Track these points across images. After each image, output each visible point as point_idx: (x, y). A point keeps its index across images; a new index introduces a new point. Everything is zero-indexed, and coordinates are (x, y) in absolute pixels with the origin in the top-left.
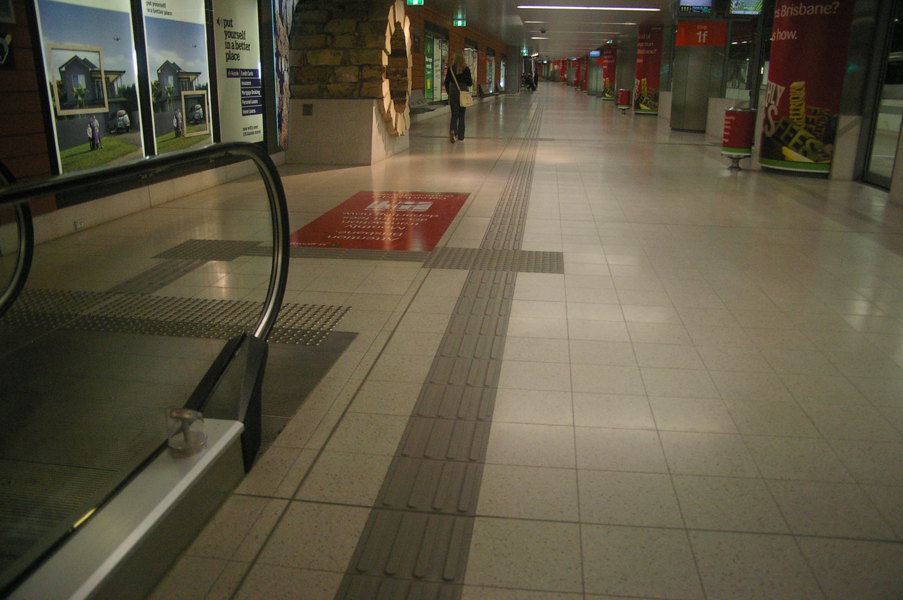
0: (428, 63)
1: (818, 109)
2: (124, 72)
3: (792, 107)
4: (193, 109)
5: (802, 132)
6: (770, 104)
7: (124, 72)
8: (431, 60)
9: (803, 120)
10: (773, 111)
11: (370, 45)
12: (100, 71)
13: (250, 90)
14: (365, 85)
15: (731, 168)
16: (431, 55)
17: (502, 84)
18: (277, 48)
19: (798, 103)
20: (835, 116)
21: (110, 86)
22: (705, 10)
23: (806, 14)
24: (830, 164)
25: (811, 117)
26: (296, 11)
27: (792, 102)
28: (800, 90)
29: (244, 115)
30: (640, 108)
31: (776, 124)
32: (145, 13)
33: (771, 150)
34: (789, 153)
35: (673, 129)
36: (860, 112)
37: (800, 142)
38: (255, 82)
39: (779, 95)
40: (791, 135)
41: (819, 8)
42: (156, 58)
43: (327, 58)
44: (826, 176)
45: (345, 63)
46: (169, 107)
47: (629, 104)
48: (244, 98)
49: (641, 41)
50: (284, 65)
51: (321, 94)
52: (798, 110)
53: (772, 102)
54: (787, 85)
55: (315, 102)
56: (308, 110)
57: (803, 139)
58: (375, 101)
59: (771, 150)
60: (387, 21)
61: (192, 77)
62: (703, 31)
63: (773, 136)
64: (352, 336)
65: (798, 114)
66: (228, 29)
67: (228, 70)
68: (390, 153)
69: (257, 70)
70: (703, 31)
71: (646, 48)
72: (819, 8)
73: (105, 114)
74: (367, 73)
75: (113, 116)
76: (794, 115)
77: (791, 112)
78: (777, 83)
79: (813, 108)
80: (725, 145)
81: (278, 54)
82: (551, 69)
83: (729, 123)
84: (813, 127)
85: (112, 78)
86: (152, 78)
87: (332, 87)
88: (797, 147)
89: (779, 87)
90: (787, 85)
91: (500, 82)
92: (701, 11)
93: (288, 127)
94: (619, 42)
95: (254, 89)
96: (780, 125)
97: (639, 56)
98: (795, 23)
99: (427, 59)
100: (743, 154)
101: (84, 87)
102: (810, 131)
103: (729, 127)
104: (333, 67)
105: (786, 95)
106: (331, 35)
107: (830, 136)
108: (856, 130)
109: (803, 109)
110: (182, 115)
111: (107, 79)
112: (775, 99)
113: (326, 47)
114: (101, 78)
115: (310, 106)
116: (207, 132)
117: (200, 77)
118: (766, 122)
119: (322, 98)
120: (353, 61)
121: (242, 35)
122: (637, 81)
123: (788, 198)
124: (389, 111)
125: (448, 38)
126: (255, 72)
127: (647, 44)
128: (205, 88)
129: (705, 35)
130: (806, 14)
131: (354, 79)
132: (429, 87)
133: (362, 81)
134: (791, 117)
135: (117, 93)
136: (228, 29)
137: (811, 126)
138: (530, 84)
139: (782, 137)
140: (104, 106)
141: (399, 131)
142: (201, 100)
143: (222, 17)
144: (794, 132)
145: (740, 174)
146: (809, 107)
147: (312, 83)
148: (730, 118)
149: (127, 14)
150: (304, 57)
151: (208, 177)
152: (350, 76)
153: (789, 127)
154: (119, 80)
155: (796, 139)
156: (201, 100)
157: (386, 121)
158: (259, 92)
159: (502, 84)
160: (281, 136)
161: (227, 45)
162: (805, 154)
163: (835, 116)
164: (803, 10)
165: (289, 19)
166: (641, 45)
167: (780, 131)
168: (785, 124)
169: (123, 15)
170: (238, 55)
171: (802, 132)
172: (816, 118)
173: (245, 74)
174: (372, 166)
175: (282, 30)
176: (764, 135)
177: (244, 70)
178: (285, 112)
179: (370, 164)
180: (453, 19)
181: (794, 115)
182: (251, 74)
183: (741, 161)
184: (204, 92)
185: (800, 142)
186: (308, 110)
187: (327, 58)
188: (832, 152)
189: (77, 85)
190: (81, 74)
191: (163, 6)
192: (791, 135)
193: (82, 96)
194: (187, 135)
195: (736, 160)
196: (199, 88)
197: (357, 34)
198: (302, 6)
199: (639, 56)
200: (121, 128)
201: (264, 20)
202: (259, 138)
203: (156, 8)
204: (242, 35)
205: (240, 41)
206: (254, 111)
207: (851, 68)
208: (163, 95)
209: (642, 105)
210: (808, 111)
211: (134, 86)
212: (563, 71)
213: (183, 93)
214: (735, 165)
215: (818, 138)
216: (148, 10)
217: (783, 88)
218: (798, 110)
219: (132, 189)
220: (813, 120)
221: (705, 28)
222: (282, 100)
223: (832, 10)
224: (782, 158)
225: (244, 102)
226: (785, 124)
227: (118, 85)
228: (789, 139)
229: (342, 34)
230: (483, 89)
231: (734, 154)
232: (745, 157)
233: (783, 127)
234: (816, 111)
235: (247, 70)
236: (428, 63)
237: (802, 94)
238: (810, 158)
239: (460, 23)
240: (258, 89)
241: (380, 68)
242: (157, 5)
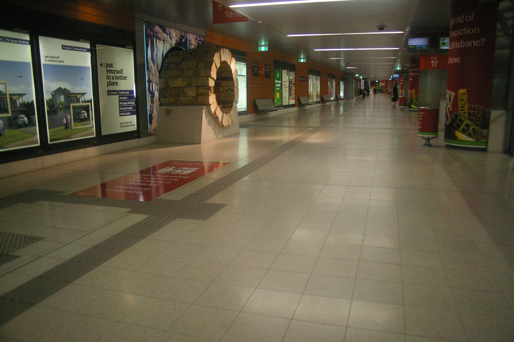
0: (278, 83)
1: (477, 106)
2: (25, 94)
3: (460, 106)
4: (79, 113)
6: (447, 104)
7: (25, 94)
8: (280, 82)
9: (467, 113)
10: (449, 108)
11: (202, 75)
12: (6, 94)
13: (127, 102)
14: (200, 97)
16: (281, 79)
17: (342, 94)
18: (149, 78)
19: (463, 103)
20: (488, 110)
21: (13, 102)
22: (424, 47)
23: (465, 47)
24: (487, 142)
25: (472, 112)
26: (165, 57)
27: (459, 102)
28: (464, 94)
29: (120, 116)
31: (451, 117)
32: (43, 61)
34: (460, 135)
36: (506, 108)
37: (466, 128)
38: (130, 98)
39: (452, 98)
40: (460, 123)
41: (472, 43)
42: (49, 86)
43: (179, 83)
44: (485, 150)
45: (189, 85)
46: (60, 113)
47: (405, 105)
48: (121, 106)
49: (411, 68)
50: (155, 87)
51: (172, 104)
52: (463, 107)
53: (449, 103)
54: (456, 91)
55: (173, 108)
56: (168, 113)
57: (467, 125)
58: (205, 107)
60: (211, 62)
61: (79, 96)
62: (435, 60)
63: (450, 125)
64: (17, 257)
65: (464, 110)
66: (109, 68)
67: (108, 91)
68: (221, 136)
69: (133, 91)
70: (435, 60)
71: (415, 72)
72: (472, 43)
73: (8, 117)
74: (201, 91)
75: (16, 118)
76: (461, 110)
77: (460, 109)
79: (473, 106)
81: (150, 81)
82: (380, 86)
83: (421, 116)
84: (474, 118)
85: (14, 98)
86: (47, 97)
87: (182, 99)
88: (464, 131)
89: (452, 93)
90: (456, 91)
91: (339, 93)
92: (421, 48)
93: (157, 122)
94: (405, 68)
95: (130, 101)
96: (453, 117)
97: (411, 77)
99: (276, 81)
100: (431, 136)
101: (63, 101)
102: (472, 120)
103: (421, 119)
104: (183, 88)
106: (182, 70)
107: (485, 124)
108: (503, 119)
110: (71, 116)
111: (11, 99)
112: (450, 101)
113: (179, 76)
114: (6, 98)
115: (170, 110)
116: (91, 126)
117: (85, 96)
119: (177, 105)
120: (193, 84)
121: (121, 71)
124: (215, 113)
125: (295, 70)
126: (131, 92)
127: (414, 70)
128: (90, 101)
129: (436, 62)
130: (465, 47)
131: (194, 94)
132: (278, 97)
133: (198, 95)
134: (459, 112)
135: (18, 105)
136: (109, 68)
137: (472, 117)
138: (363, 94)
140: (8, 112)
141: (225, 123)
142: (87, 108)
143: (105, 62)
144: (462, 122)
145: (431, 148)
146: (471, 105)
147: (171, 97)
148: (422, 113)
149: (30, 63)
150: (167, 83)
151: (92, 151)
152: (192, 92)
153: (458, 119)
154: (83, 97)
155: (463, 126)
156: (87, 108)
157: (214, 117)
158: (134, 103)
159: (342, 94)
160: (152, 127)
161: (108, 78)
162: (469, 135)
163: (488, 110)
164: (463, 44)
165: (160, 62)
166: (411, 70)
167: (454, 121)
168: (456, 116)
169: (21, 65)
170: (117, 83)
171: (467, 121)
172: (475, 112)
173: (121, 93)
174: (202, 145)
175: (154, 68)
176: (446, 123)
177: (121, 91)
178: (155, 113)
179: (200, 143)
180: (298, 58)
181: (461, 110)
182: (128, 93)
183: (431, 140)
184: (89, 104)
185: (466, 128)
186: (168, 113)
187: (179, 83)
188: (488, 134)
189: (59, 100)
190: (62, 95)
191: (58, 58)
192: (460, 123)
193: (62, 105)
194: (73, 128)
195: (428, 139)
196: (85, 102)
197: (196, 69)
198: (170, 54)
199: (411, 77)
200: (21, 125)
201: (138, 63)
202: (134, 128)
203: (52, 59)
204: (121, 71)
205: (118, 75)
206: (130, 113)
207: (496, 81)
208: (55, 106)
209: (413, 106)
210: (470, 108)
211: (33, 102)
212: (386, 86)
213: (71, 105)
214: (427, 143)
215: (477, 125)
216: (46, 60)
217: (454, 94)
218: (463, 107)
219: (30, 158)
220: (474, 113)
221: (436, 58)
222: (153, 107)
223: (481, 43)
224: (455, 138)
225: (121, 109)
226: (456, 116)
227: (19, 101)
228: (459, 126)
229: (188, 69)
230: (325, 97)
231: (426, 136)
232: (433, 138)
233: (454, 118)
234: (475, 108)
235: (124, 91)
236: (278, 83)
237: (466, 97)
238: (473, 138)
239: (302, 61)
240: (133, 101)
241: (209, 88)
242: (52, 57)
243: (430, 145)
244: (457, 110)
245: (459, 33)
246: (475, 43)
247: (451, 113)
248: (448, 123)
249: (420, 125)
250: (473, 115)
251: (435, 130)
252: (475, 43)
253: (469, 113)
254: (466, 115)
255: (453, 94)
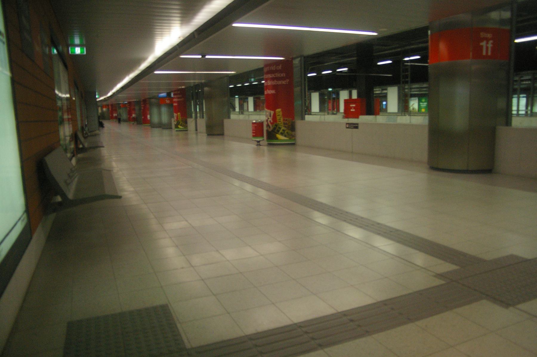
5: (283, 128)
15: (257, 145)
30: (178, 128)
33: (271, 136)
35: (208, 135)
39: (272, 114)
44: (294, 144)
57: (284, 130)
59: (271, 136)
63: (272, 131)
78: (271, 110)
80: (254, 136)
84: (287, 126)
88: (282, 134)
90: (274, 109)
97: (175, 102)
98: (274, 87)
102: (286, 127)
105: (275, 115)
109: (282, 119)
118: (268, 125)
122: (175, 115)
123: (282, 153)
139: (276, 131)
144: (280, 128)
155: (281, 131)
162: (285, 136)
167: (275, 129)
168: (276, 126)
171: (283, 128)
176: (267, 131)
195: (259, 142)
199: (175, 102)
209: (180, 127)
210: (284, 120)
224: (277, 139)
228: (278, 131)
231: (258, 139)
237: (281, 113)
243: (260, 145)
244: (276, 121)
245: (273, 76)
246: (284, 82)
247: (271, 123)
248: (270, 130)
249: (253, 133)
250: (286, 124)
251: (262, 135)
252: (284, 82)
253: (284, 124)
254: (282, 124)
255: (272, 112)
